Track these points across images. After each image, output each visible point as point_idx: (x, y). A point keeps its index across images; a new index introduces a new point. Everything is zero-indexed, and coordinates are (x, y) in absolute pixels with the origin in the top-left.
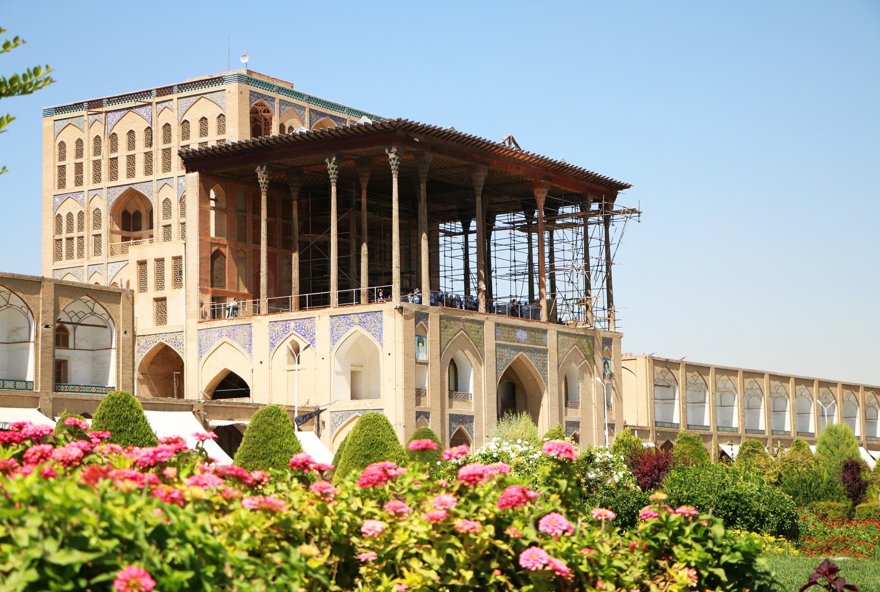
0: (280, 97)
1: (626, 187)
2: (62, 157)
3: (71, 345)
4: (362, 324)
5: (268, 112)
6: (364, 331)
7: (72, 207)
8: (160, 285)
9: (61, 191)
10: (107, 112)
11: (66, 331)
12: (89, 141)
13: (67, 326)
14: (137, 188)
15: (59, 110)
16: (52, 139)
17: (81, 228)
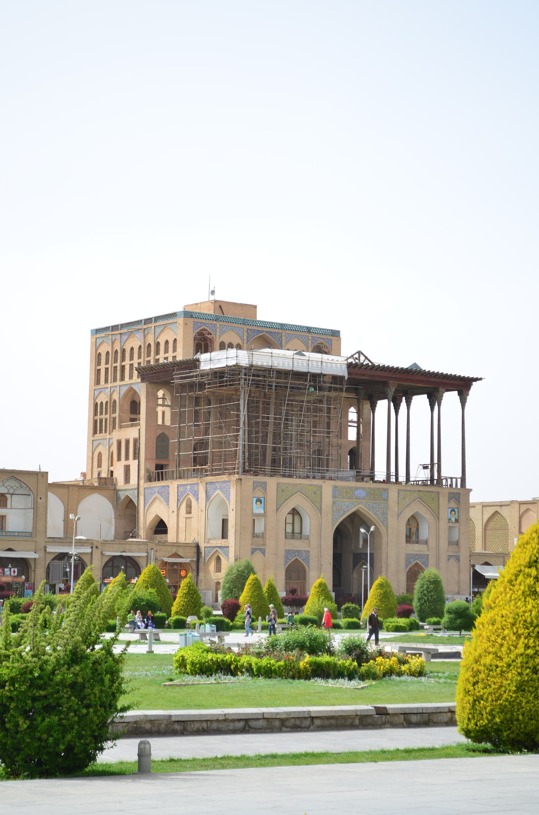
0: (218, 324)
1: (481, 379)
2: (99, 363)
3: (9, 506)
4: (221, 489)
5: (211, 334)
6: (222, 495)
7: (103, 398)
8: (127, 458)
9: (98, 387)
10: (121, 334)
11: (6, 497)
12: (112, 353)
13: (7, 495)
14: (134, 386)
15: (98, 331)
16: (94, 351)
17: (106, 413)
